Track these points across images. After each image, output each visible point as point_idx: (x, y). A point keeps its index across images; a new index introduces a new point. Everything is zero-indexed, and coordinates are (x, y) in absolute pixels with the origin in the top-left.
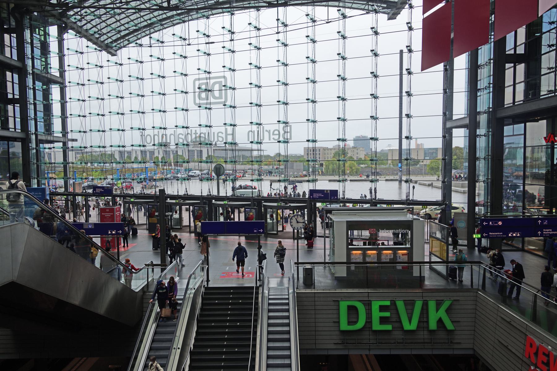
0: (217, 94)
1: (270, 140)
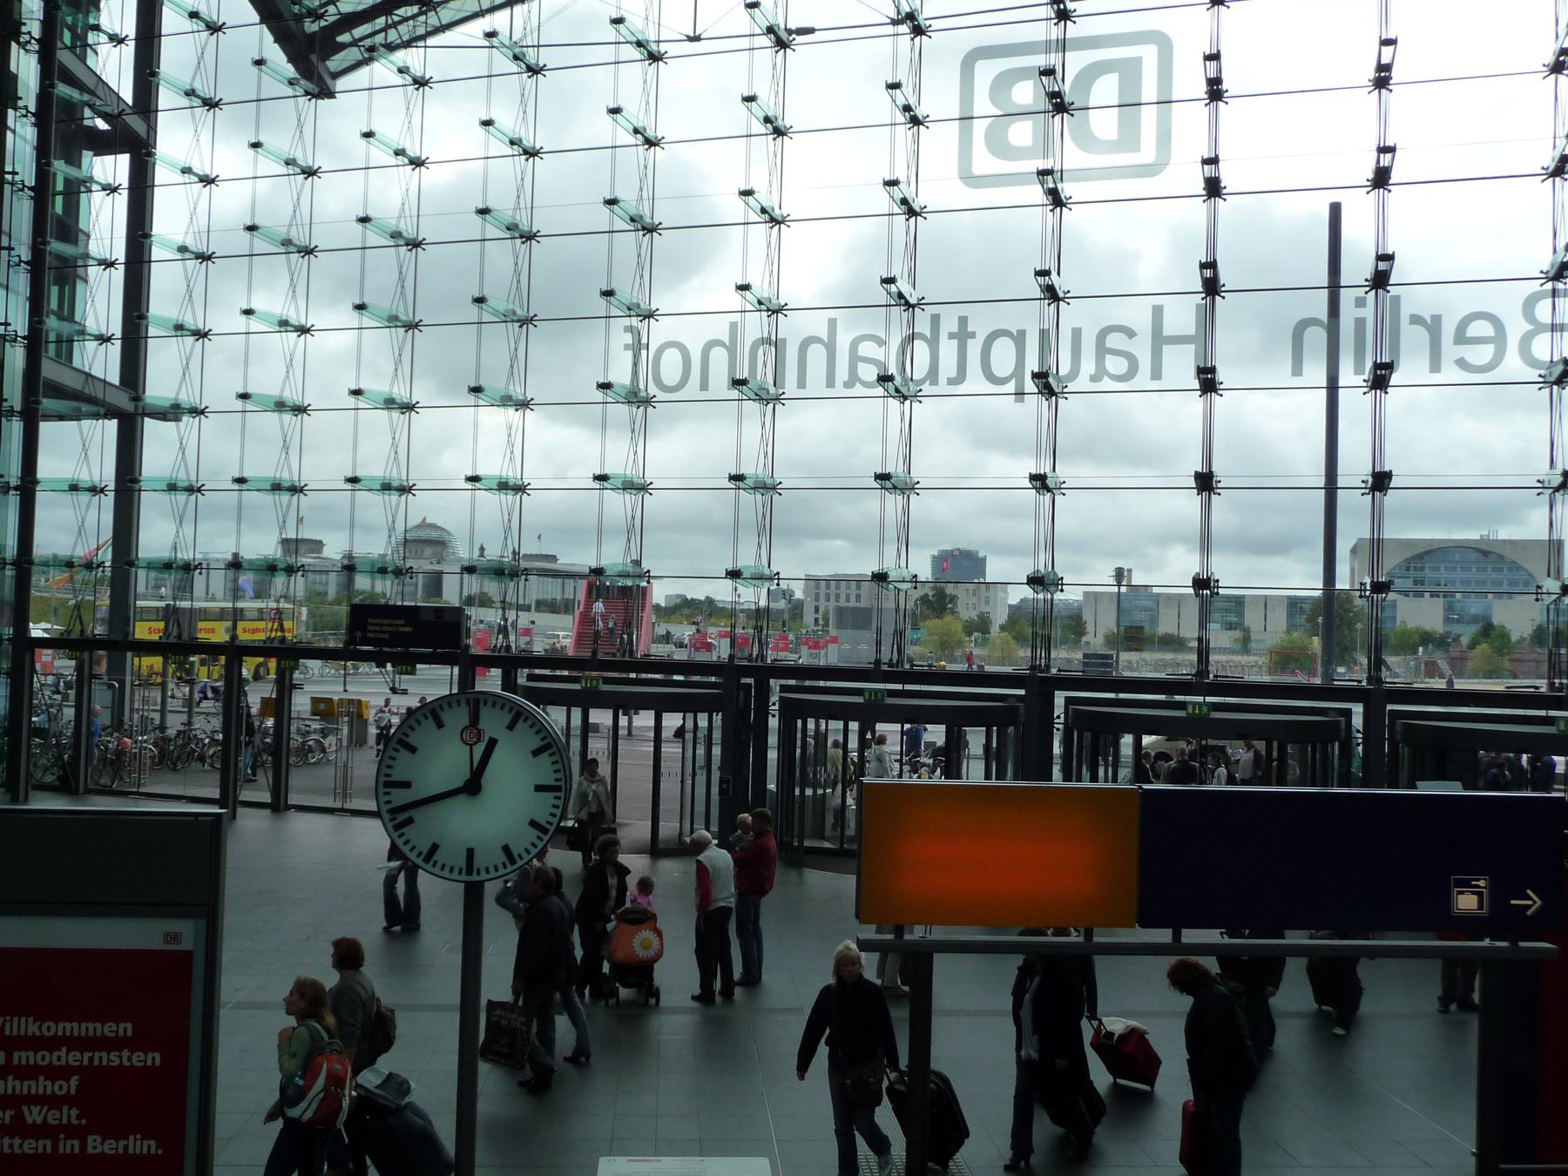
0: (1104, 124)
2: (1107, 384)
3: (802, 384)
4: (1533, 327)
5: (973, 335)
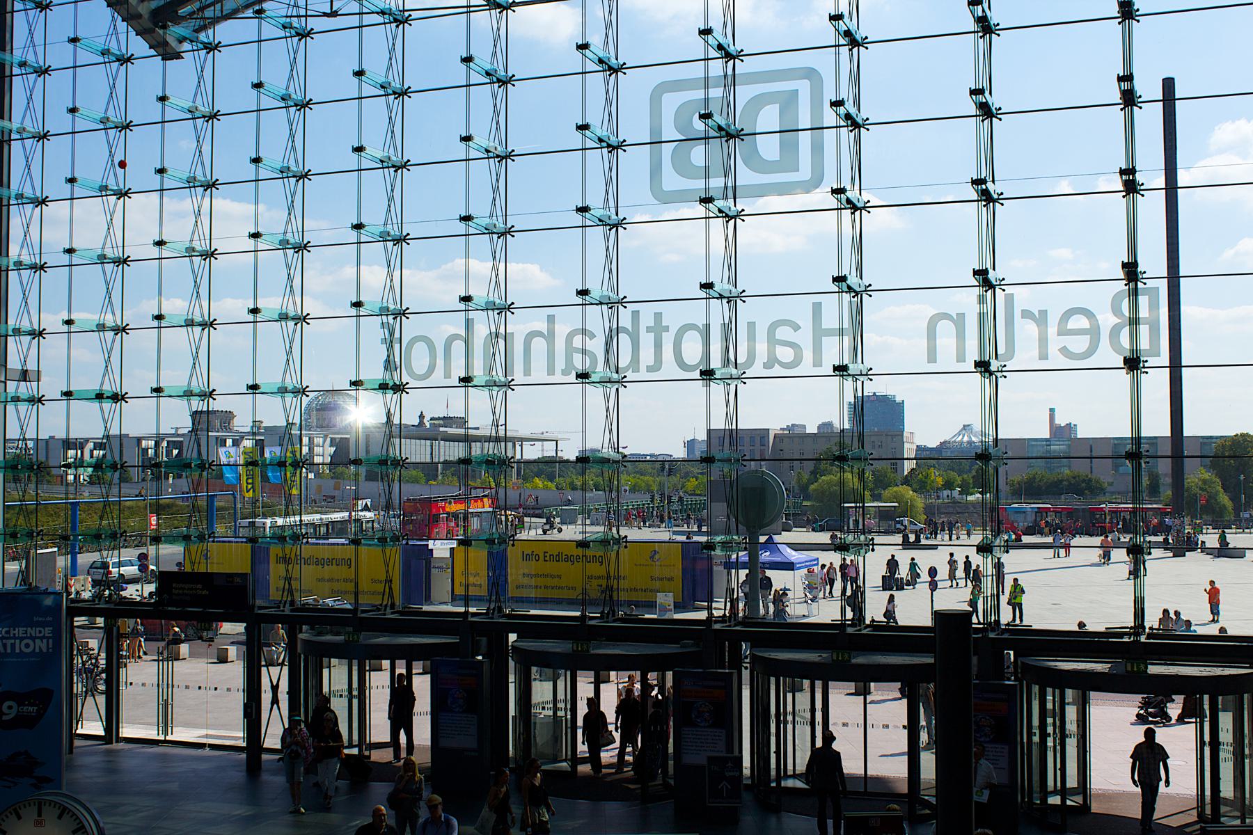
0: (769, 147)
1: (1043, 356)
2: (777, 370)
3: (527, 372)
4: (1120, 321)
5: (667, 329)
